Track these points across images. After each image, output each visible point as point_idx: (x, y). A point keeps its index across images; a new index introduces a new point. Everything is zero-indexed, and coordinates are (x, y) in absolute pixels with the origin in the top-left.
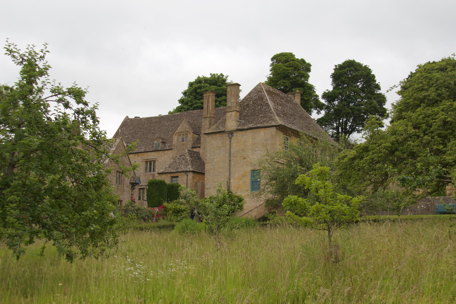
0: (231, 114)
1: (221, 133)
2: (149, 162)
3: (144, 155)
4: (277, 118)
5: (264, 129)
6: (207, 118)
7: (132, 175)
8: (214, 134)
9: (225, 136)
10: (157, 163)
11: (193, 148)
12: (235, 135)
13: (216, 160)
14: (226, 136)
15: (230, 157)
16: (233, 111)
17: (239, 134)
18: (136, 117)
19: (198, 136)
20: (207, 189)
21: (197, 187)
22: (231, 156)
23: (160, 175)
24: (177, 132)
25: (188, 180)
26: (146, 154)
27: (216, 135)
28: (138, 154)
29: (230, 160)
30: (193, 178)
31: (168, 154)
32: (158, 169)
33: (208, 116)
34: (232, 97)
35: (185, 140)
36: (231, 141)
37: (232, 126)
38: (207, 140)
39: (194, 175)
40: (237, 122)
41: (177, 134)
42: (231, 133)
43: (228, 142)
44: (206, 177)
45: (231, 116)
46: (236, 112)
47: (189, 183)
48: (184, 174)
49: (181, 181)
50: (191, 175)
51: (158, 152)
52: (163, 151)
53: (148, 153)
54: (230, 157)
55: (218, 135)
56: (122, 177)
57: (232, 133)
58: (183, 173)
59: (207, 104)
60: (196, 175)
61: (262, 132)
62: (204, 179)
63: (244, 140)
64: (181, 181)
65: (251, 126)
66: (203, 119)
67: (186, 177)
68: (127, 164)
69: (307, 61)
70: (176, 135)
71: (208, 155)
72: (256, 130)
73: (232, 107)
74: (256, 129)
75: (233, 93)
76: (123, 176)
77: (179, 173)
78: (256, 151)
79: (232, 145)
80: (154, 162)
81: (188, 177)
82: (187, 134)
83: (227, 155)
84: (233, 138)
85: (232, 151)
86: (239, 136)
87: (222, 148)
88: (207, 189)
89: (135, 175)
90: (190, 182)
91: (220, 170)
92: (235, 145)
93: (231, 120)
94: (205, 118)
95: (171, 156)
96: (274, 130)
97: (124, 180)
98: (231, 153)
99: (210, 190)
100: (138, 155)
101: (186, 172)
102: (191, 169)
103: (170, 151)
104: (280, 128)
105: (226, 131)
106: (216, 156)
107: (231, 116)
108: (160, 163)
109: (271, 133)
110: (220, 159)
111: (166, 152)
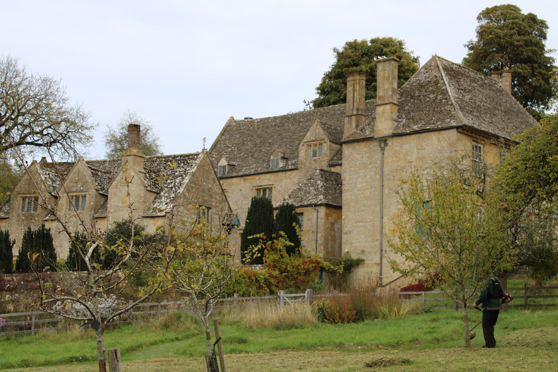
0: (384, 110)
1: (368, 140)
2: (262, 190)
3: (255, 178)
4: (460, 114)
5: (436, 133)
6: (353, 117)
7: (227, 211)
8: (356, 144)
9: (374, 146)
10: (274, 192)
11: (331, 166)
12: (390, 143)
13: (359, 186)
14: (374, 145)
15: (382, 180)
16: (386, 104)
17: (397, 140)
18: (246, 118)
19: (339, 146)
20: (346, 233)
21: (334, 230)
22: (384, 178)
24: (306, 141)
25: (319, 220)
26: (257, 177)
27: (360, 144)
28: (245, 177)
30: (327, 215)
31: (292, 177)
32: (275, 201)
33: (355, 113)
34: (386, 81)
35: (317, 153)
37: (385, 129)
38: (346, 152)
39: (328, 211)
40: (394, 122)
41: (305, 144)
42: (384, 140)
43: (380, 155)
44: (343, 213)
45: (383, 112)
46: (391, 104)
47: (320, 224)
48: (313, 209)
49: (308, 220)
50: (323, 211)
51: (276, 174)
52: (284, 173)
53: (261, 176)
54: (382, 180)
55: (362, 145)
56: (208, 215)
57: (386, 140)
58: (310, 208)
59: (352, 94)
60: (332, 210)
61: (434, 137)
62: (341, 217)
63: (404, 151)
64: (308, 220)
65: (416, 128)
66: (347, 119)
67: (315, 214)
68: (216, 194)
69: (540, 17)
70: (303, 145)
71: (348, 178)
72: (424, 135)
73: (386, 98)
74: (424, 132)
75: (387, 75)
76: (210, 213)
77: (304, 208)
79: (385, 159)
80: (270, 189)
81: (319, 214)
82: (321, 144)
83: (378, 176)
84: (387, 148)
85: (386, 169)
86: (397, 146)
87: (370, 167)
88: (346, 233)
89: (232, 212)
90: (322, 221)
91: (366, 202)
92: (390, 160)
93: (383, 119)
94: (349, 116)
95: (296, 180)
96: (453, 133)
97: (211, 220)
98: (385, 174)
99: (350, 236)
100: (245, 180)
101: (316, 205)
102: (324, 201)
103: (295, 172)
104: (464, 130)
105: (376, 137)
106: (359, 180)
108: (279, 191)
109: (449, 140)
110: (366, 184)
111: (289, 173)
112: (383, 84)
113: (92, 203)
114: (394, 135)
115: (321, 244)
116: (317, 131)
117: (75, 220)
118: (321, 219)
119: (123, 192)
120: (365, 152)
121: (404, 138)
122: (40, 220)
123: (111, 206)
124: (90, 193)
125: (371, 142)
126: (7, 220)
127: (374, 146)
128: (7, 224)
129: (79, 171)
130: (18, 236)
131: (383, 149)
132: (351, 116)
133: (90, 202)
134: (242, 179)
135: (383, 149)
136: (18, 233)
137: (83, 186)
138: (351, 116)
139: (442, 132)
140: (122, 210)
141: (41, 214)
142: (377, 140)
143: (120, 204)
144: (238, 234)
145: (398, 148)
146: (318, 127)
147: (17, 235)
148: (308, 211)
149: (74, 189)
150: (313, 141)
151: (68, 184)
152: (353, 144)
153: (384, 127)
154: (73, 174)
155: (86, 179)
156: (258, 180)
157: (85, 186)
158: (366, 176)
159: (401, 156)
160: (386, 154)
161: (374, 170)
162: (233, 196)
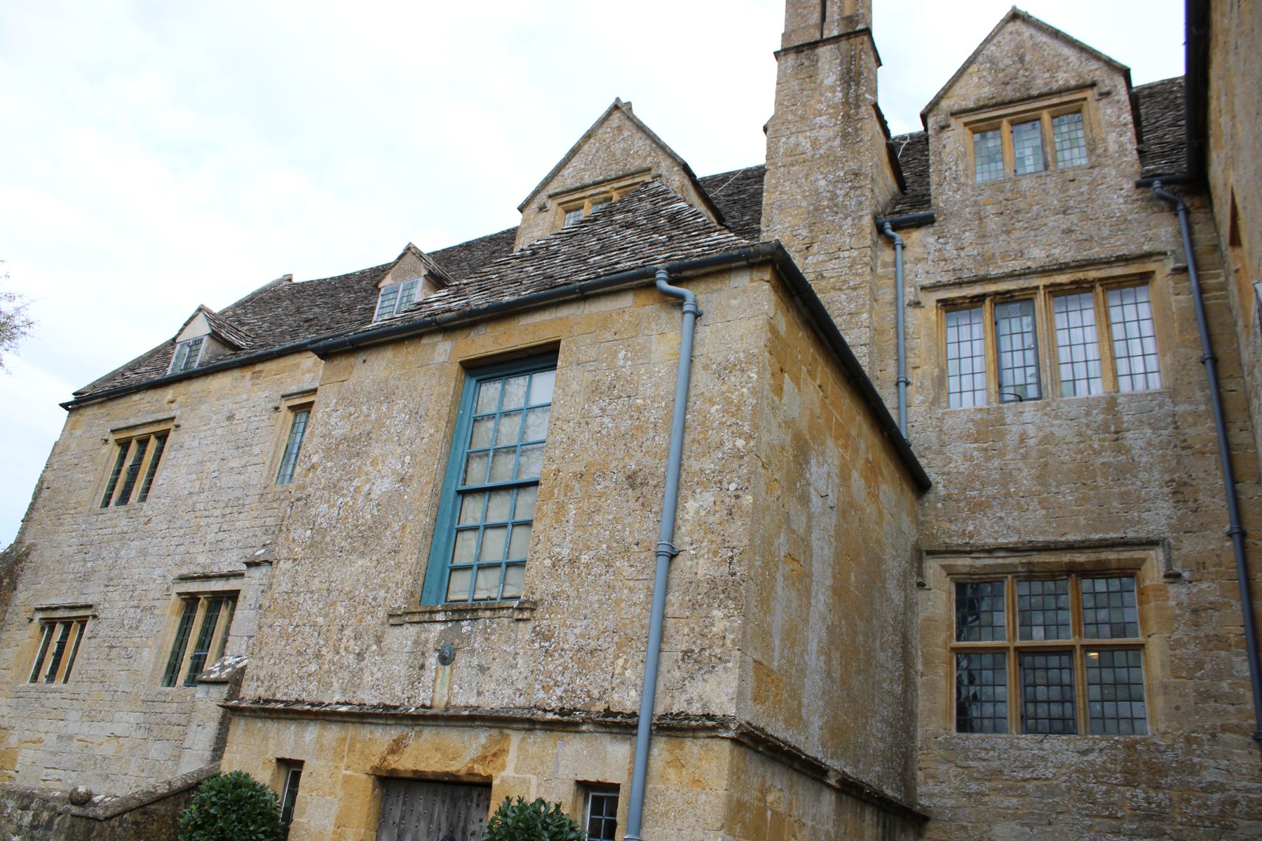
6: (824, 52)
23: (342, 362)
25: (702, 378)
41: (552, 205)
70: (542, 209)
115: (723, 590)
116: (618, 148)
118: (723, 371)
132: (813, 45)
134: (248, 373)
138: (813, 45)
144: (174, 597)
146: (626, 133)
148: (606, 321)
150: (597, 184)
156: (309, 371)
162: (195, 444)
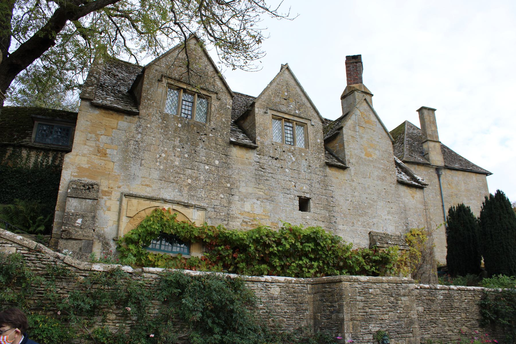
5: (474, 174)
27: (420, 167)
29: (443, 206)
36: (439, 180)
42: (438, 169)
43: (437, 180)
72: (466, 173)
73: (434, 137)
78: (471, 200)
79: (442, 185)
83: (438, 197)
86: (449, 177)
93: (435, 153)
107: (434, 146)
112: (430, 126)
113: (319, 141)
114: (446, 168)
117: (294, 159)
119: (364, 139)
120: (425, 174)
121: (453, 172)
122: (220, 140)
123: (351, 155)
124: (313, 124)
125: (428, 168)
126: (135, 119)
127: (432, 171)
128: (134, 126)
129: (287, 84)
130: (165, 158)
131: (439, 176)
133: (316, 139)
135: (439, 176)
136: (166, 152)
137: (299, 109)
139: (478, 175)
140: (368, 165)
141: (219, 129)
142: (433, 168)
143: (363, 155)
145: (450, 178)
147: (163, 155)
149: (284, 109)
151: (270, 96)
152: (414, 166)
153: (437, 159)
154: (278, 84)
155: (301, 100)
157: (302, 110)
158: (428, 194)
159: (453, 185)
160: (441, 181)
161: (435, 191)
